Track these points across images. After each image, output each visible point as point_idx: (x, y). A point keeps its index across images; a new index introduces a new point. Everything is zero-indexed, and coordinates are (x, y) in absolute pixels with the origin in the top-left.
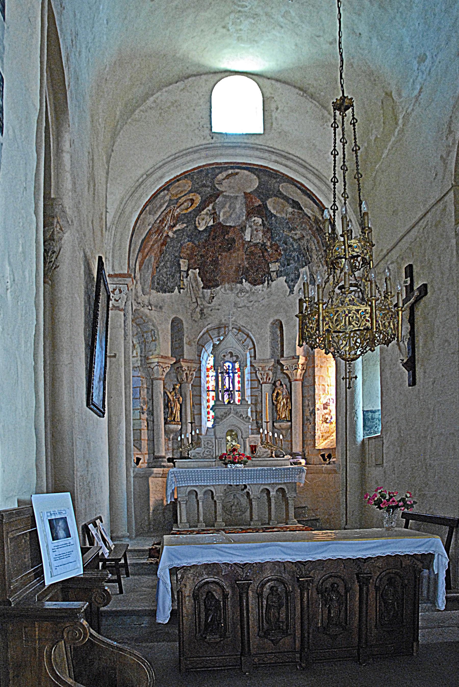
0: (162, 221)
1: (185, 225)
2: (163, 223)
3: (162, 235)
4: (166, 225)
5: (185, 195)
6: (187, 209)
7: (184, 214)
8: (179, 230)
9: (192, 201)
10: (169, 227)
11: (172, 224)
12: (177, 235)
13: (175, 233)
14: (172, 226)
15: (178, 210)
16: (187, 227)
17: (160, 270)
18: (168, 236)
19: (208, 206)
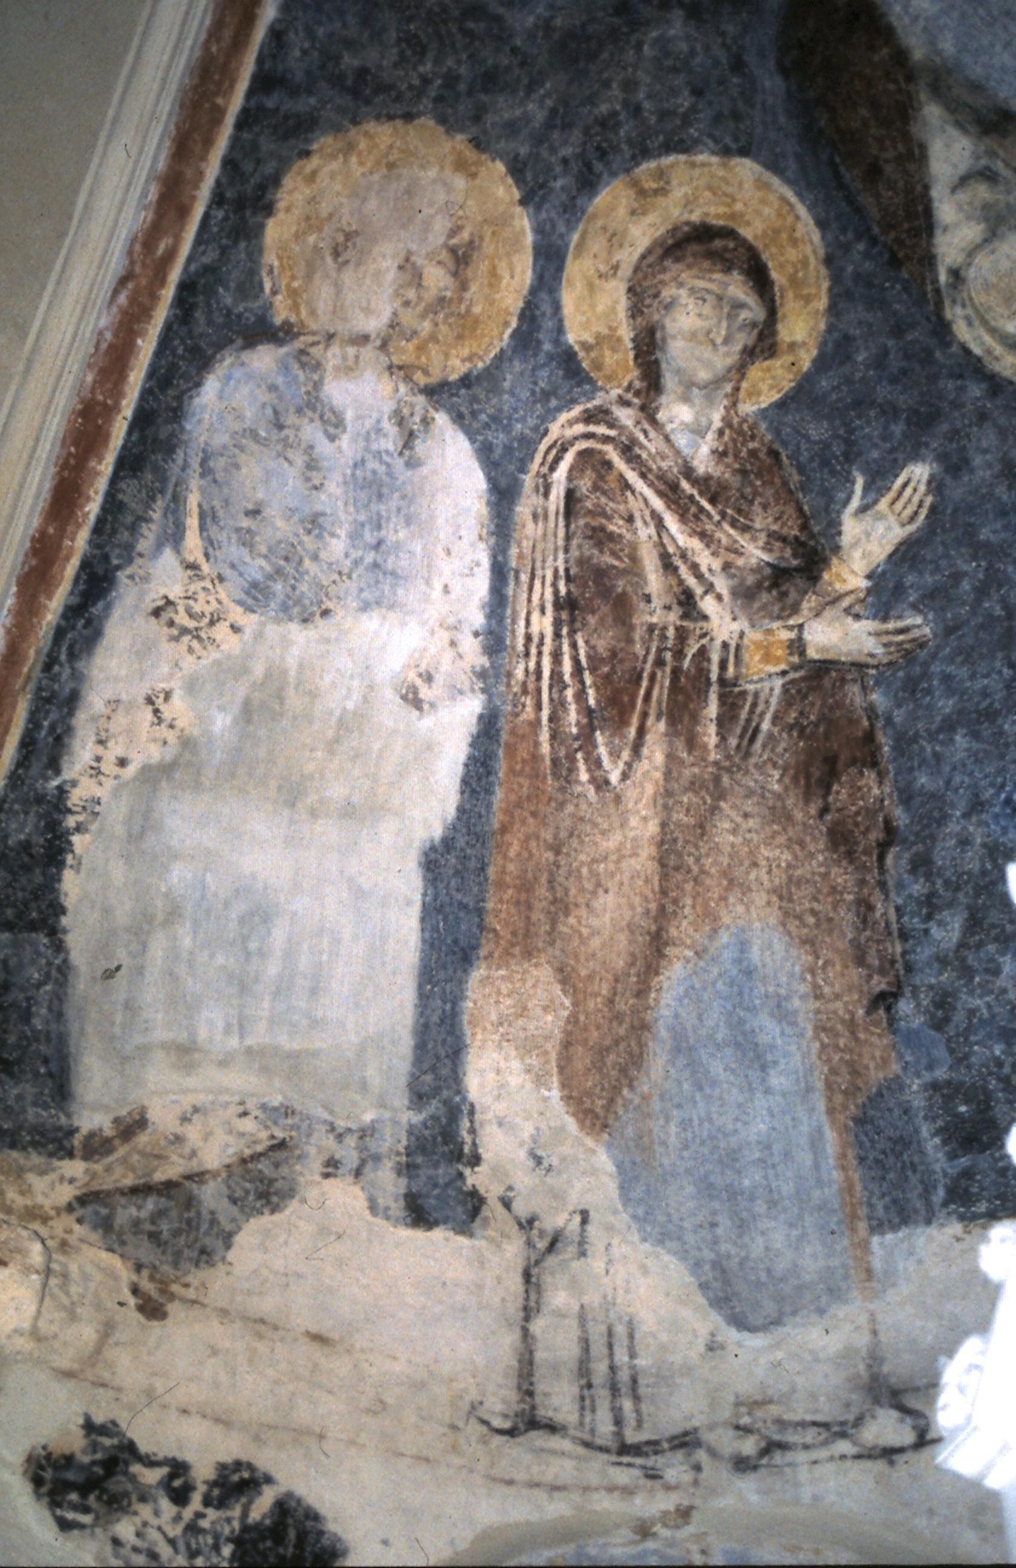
0: (594, 592)
1: (919, 472)
2: (622, 609)
3: (732, 699)
4: (687, 602)
5: (550, 259)
6: (764, 343)
7: (800, 397)
8: (906, 554)
9: (702, 243)
10: (745, 595)
11: (755, 553)
12: (933, 599)
13: (885, 593)
14: (777, 577)
15: (677, 413)
16: (953, 465)
17: (944, 1002)
18: (817, 676)
19: (915, 155)
